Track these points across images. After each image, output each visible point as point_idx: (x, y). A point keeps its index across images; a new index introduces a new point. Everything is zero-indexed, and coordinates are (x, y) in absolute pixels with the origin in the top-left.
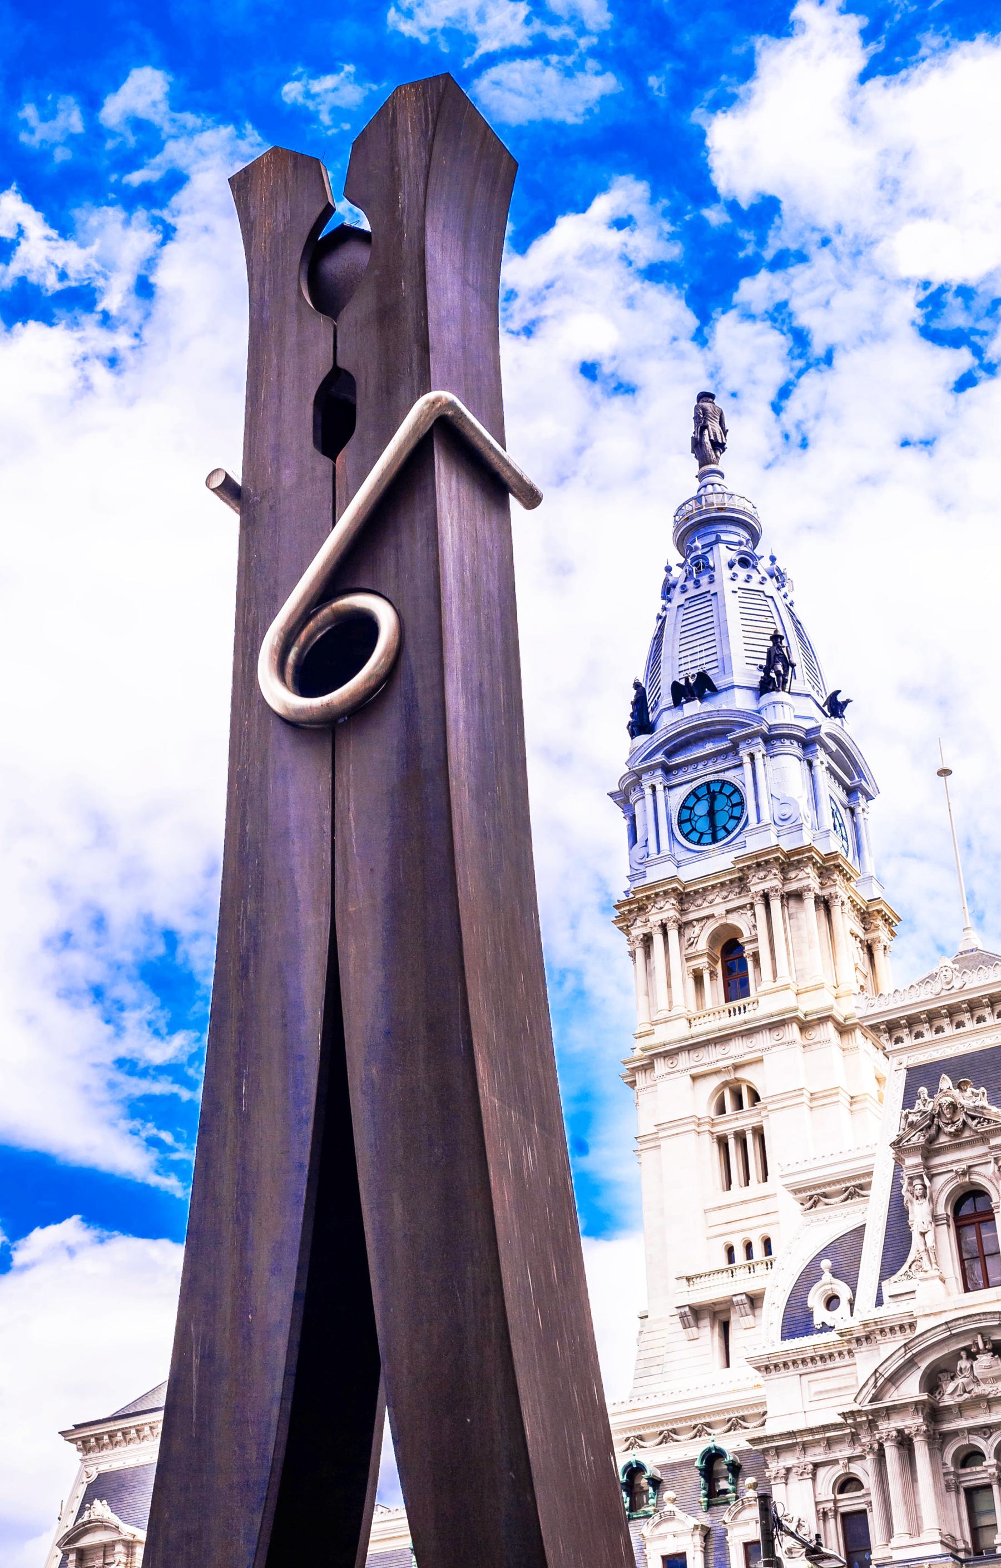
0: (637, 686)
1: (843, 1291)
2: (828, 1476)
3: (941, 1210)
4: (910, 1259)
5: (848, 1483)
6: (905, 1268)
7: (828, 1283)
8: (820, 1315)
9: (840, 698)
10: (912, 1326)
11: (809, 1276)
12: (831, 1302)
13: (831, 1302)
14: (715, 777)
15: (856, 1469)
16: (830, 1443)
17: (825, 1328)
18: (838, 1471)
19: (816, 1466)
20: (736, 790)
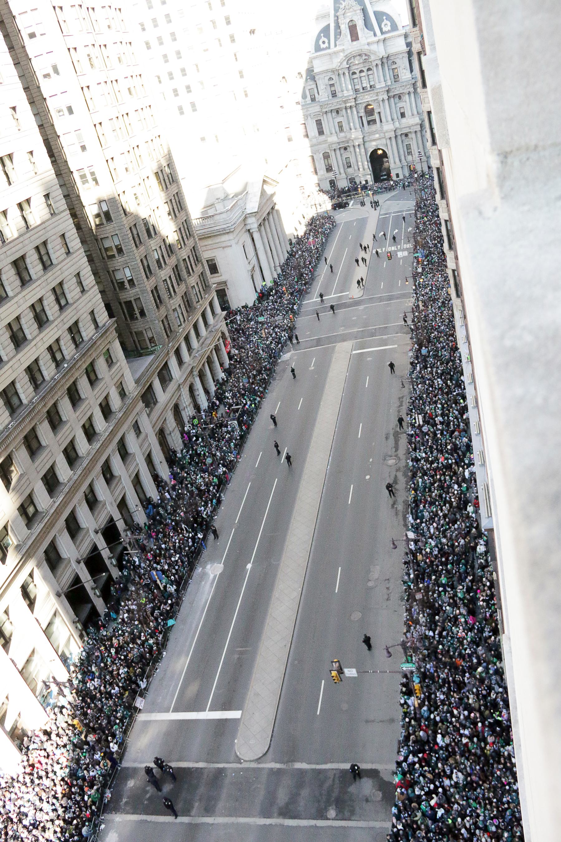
1: (326, 41)
3: (347, 26)
5: (331, 79)
7: (323, 39)
11: (319, 37)
12: (324, 42)
13: (324, 42)
15: (331, 76)
17: (324, 49)
18: (329, 77)
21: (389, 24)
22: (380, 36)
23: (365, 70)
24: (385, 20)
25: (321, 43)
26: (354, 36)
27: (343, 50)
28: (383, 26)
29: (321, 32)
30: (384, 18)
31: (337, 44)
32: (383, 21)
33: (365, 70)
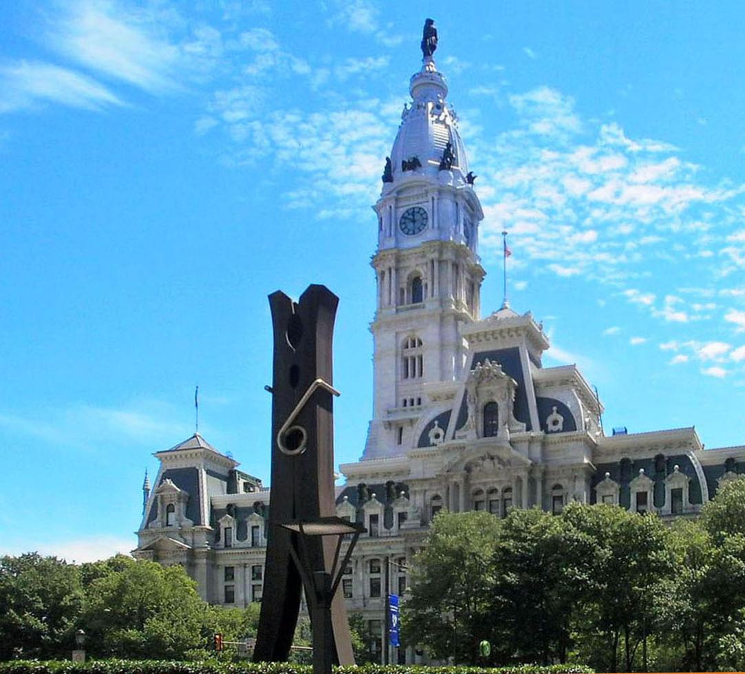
0: (387, 159)
1: (441, 432)
2: (429, 495)
4: (467, 424)
5: (436, 497)
6: (465, 427)
7: (437, 429)
8: (432, 440)
9: (473, 175)
10: (464, 448)
11: (430, 425)
12: (437, 436)
14: (417, 206)
16: (431, 485)
17: (434, 445)
18: (434, 493)
19: (425, 491)
20: (425, 212)
21: (561, 419)
22: (537, 432)
23: (499, 488)
24: (555, 413)
25: (431, 434)
26: (490, 429)
27: (463, 448)
28: (549, 421)
29: (437, 418)
30: (555, 408)
31: (456, 435)
32: (552, 412)
33: (499, 488)
